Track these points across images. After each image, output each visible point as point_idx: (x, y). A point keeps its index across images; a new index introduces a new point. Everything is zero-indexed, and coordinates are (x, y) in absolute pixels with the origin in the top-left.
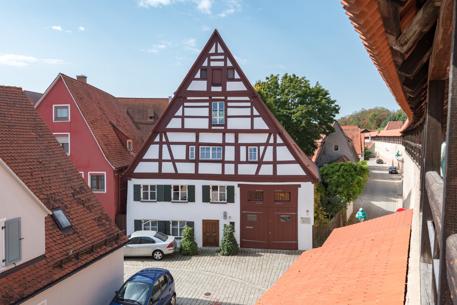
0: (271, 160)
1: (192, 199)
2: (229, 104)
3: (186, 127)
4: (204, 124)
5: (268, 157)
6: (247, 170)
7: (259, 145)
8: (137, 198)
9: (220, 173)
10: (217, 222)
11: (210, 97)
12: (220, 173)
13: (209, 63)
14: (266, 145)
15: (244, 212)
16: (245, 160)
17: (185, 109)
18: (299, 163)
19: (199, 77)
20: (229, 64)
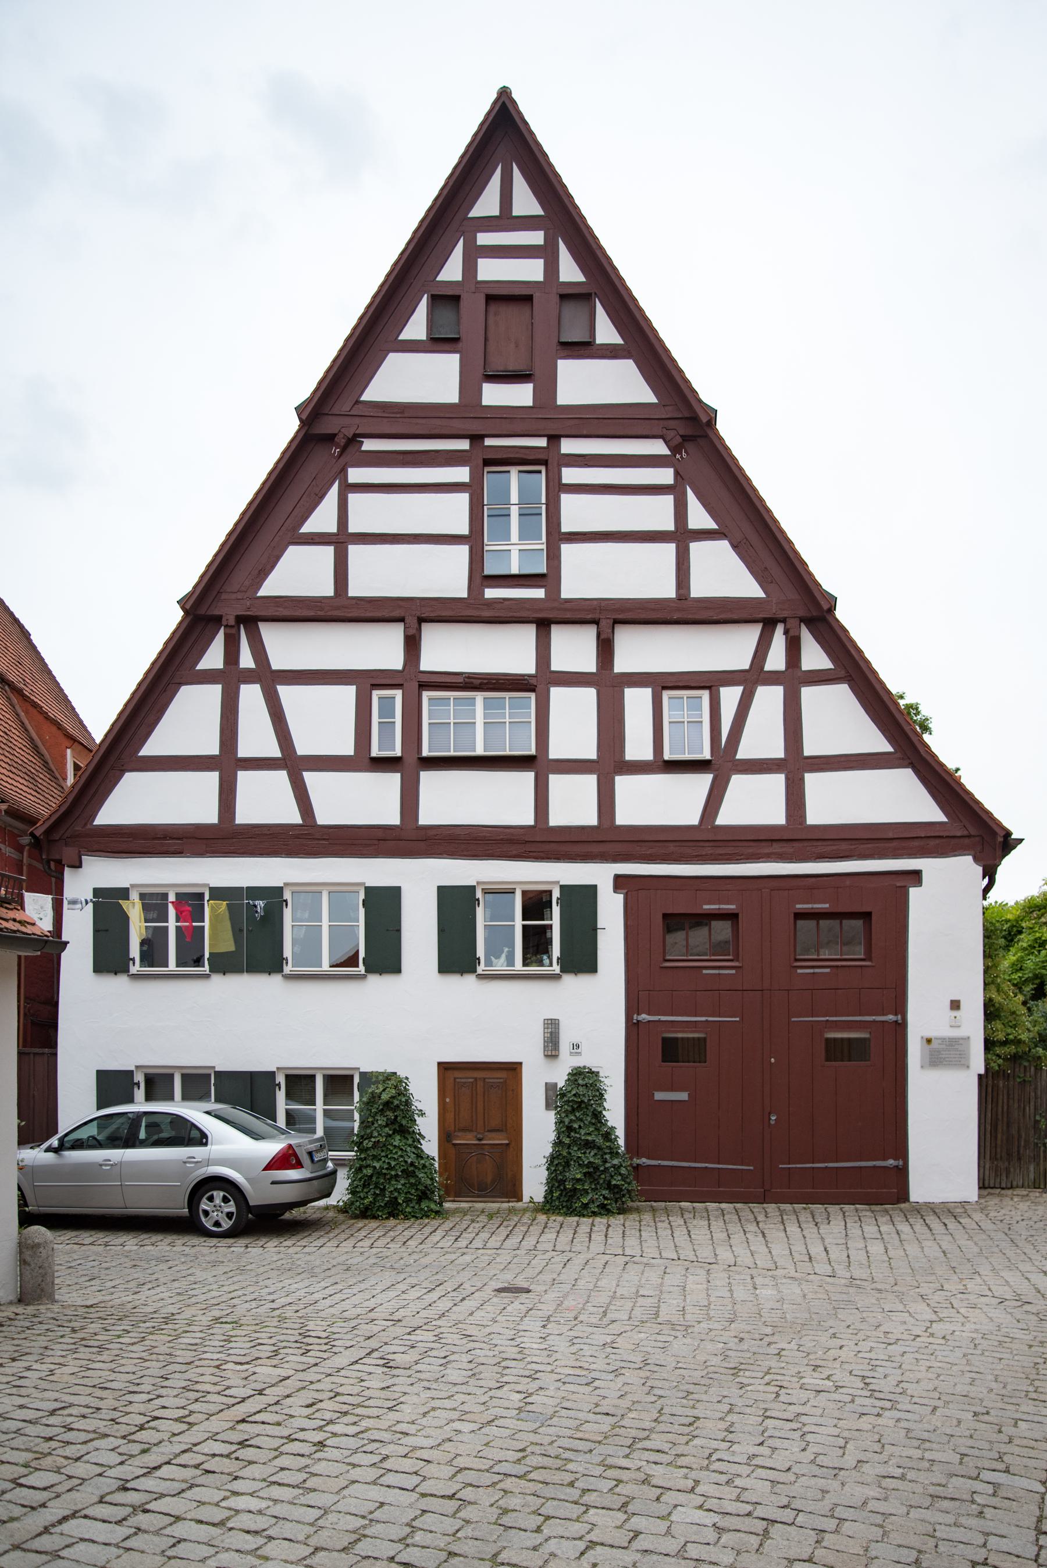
0: (777, 751)
1: (383, 955)
5: (763, 737)
6: (657, 802)
9: (528, 818)
10: (514, 1069)
11: (476, 439)
12: (528, 818)
14: (753, 677)
15: (644, 1017)
16: (648, 755)
17: (353, 498)
20: (570, 272)
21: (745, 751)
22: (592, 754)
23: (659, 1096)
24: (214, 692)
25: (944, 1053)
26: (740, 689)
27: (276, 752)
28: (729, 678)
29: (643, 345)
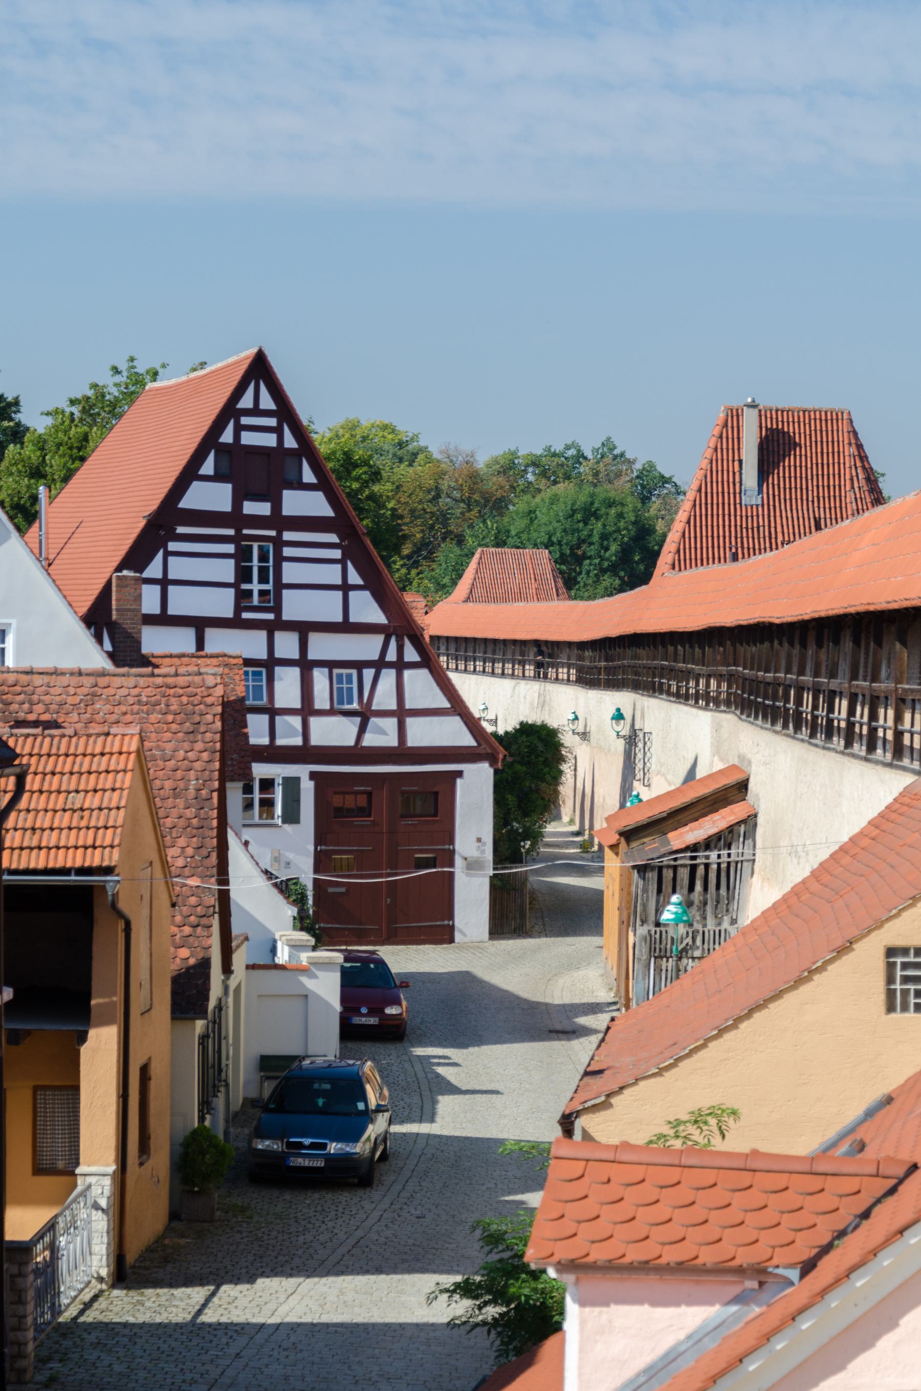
2: (287, 552)
3: (171, 611)
4: (221, 604)
5: (385, 697)
6: (332, 732)
7: (359, 666)
11: (238, 531)
13: (237, 436)
14: (379, 665)
17: (170, 559)
18: (460, 715)
20: (290, 442)
25: (473, 865)
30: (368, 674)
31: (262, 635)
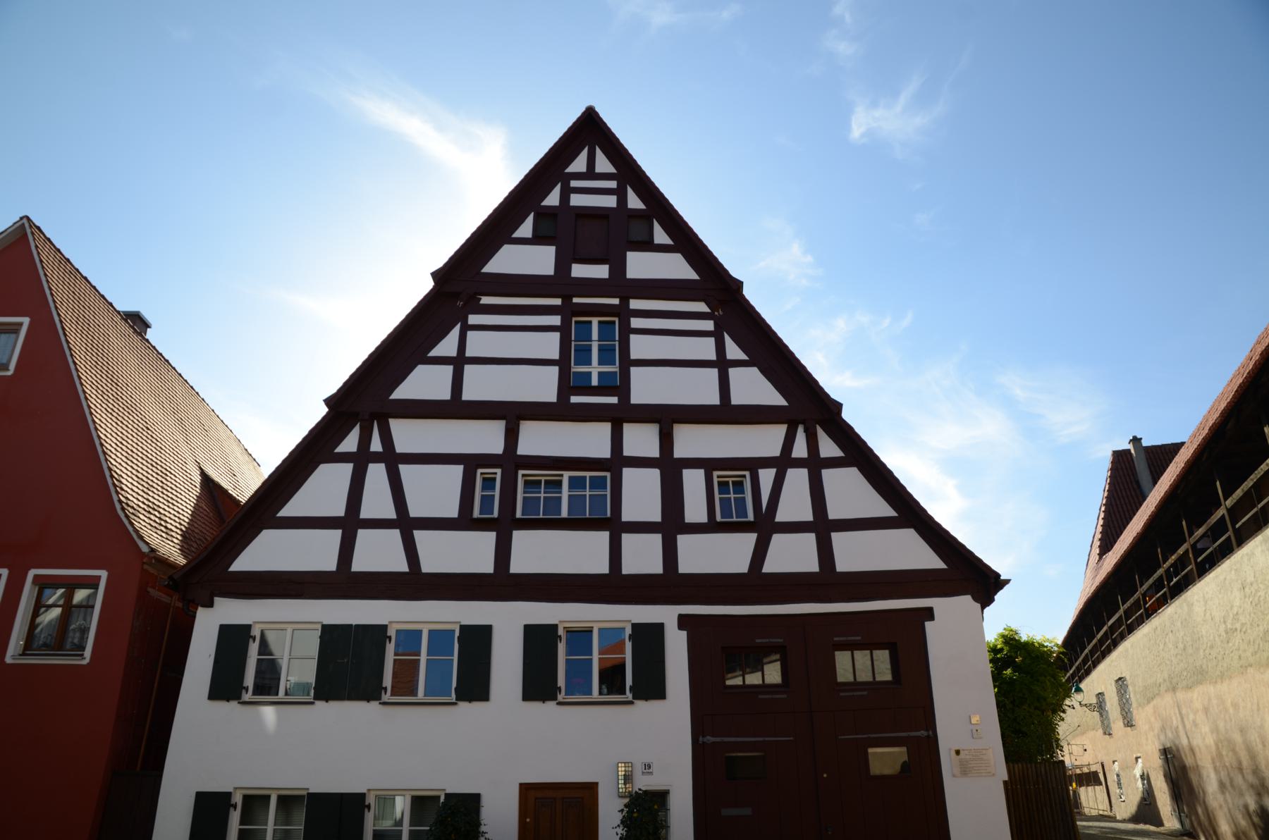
0: (808, 516)
4: (542, 386)
7: (753, 465)
8: (225, 686)
11: (567, 298)
13: (565, 197)
14: (783, 462)
15: (709, 739)
17: (470, 334)
19: (530, 235)
20: (634, 202)
21: (782, 516)
22: (657, 517)
23: (726, 812)
24: (348, 468)
26: (774, 471)
27: (392, 514)
28: (766, 462)
29: (687, 242)
30: (767, 477)
31: (605, 429)
